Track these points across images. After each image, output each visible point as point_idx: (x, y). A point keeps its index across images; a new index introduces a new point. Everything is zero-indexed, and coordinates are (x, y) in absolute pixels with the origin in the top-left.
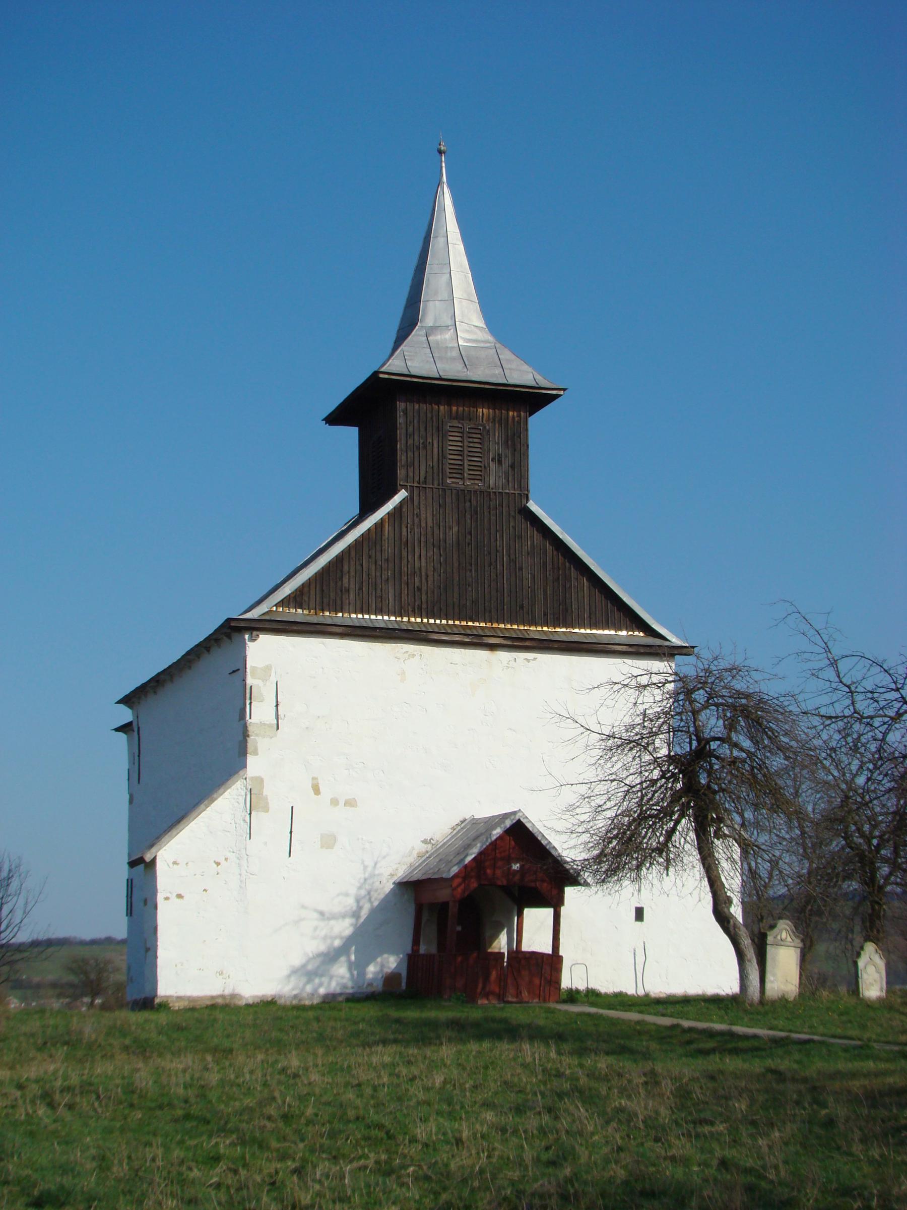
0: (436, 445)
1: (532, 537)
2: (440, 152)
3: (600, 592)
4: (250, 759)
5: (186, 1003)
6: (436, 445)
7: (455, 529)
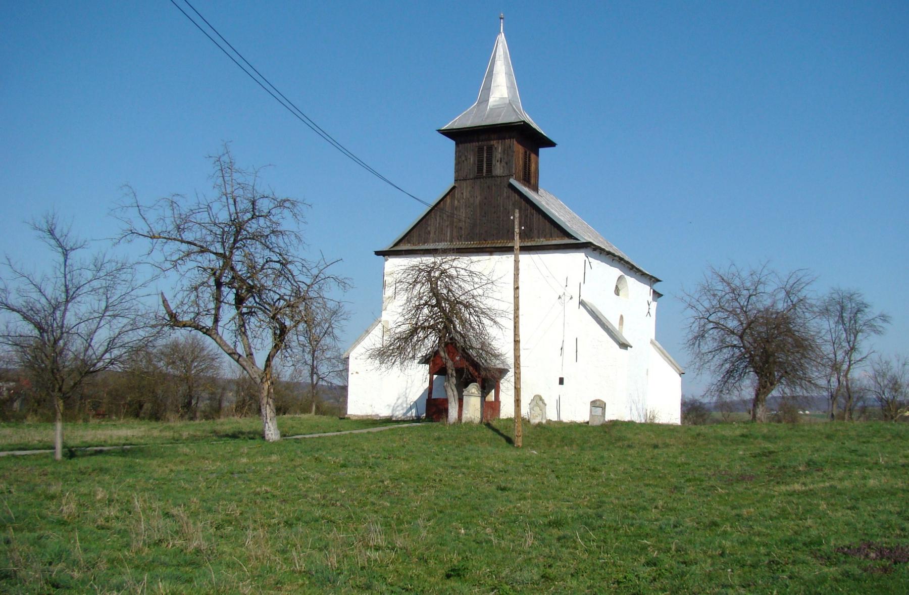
0: (472, 159)
1: (515, 196)
2: (501, 18)
3: (548, 221)
4: (384, 313)
5: (357, 418)
6: (472, 159)
7: (479, 198)
